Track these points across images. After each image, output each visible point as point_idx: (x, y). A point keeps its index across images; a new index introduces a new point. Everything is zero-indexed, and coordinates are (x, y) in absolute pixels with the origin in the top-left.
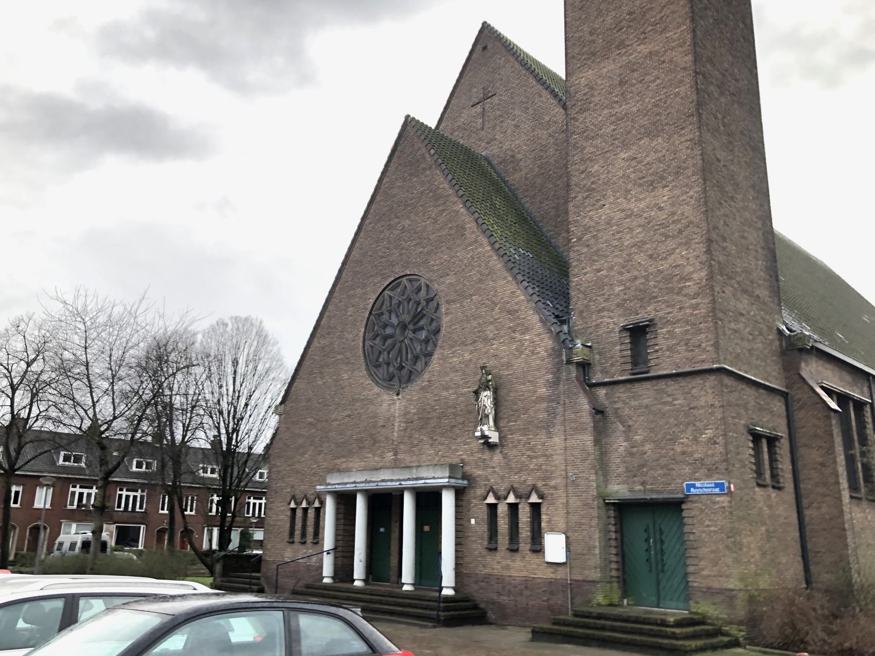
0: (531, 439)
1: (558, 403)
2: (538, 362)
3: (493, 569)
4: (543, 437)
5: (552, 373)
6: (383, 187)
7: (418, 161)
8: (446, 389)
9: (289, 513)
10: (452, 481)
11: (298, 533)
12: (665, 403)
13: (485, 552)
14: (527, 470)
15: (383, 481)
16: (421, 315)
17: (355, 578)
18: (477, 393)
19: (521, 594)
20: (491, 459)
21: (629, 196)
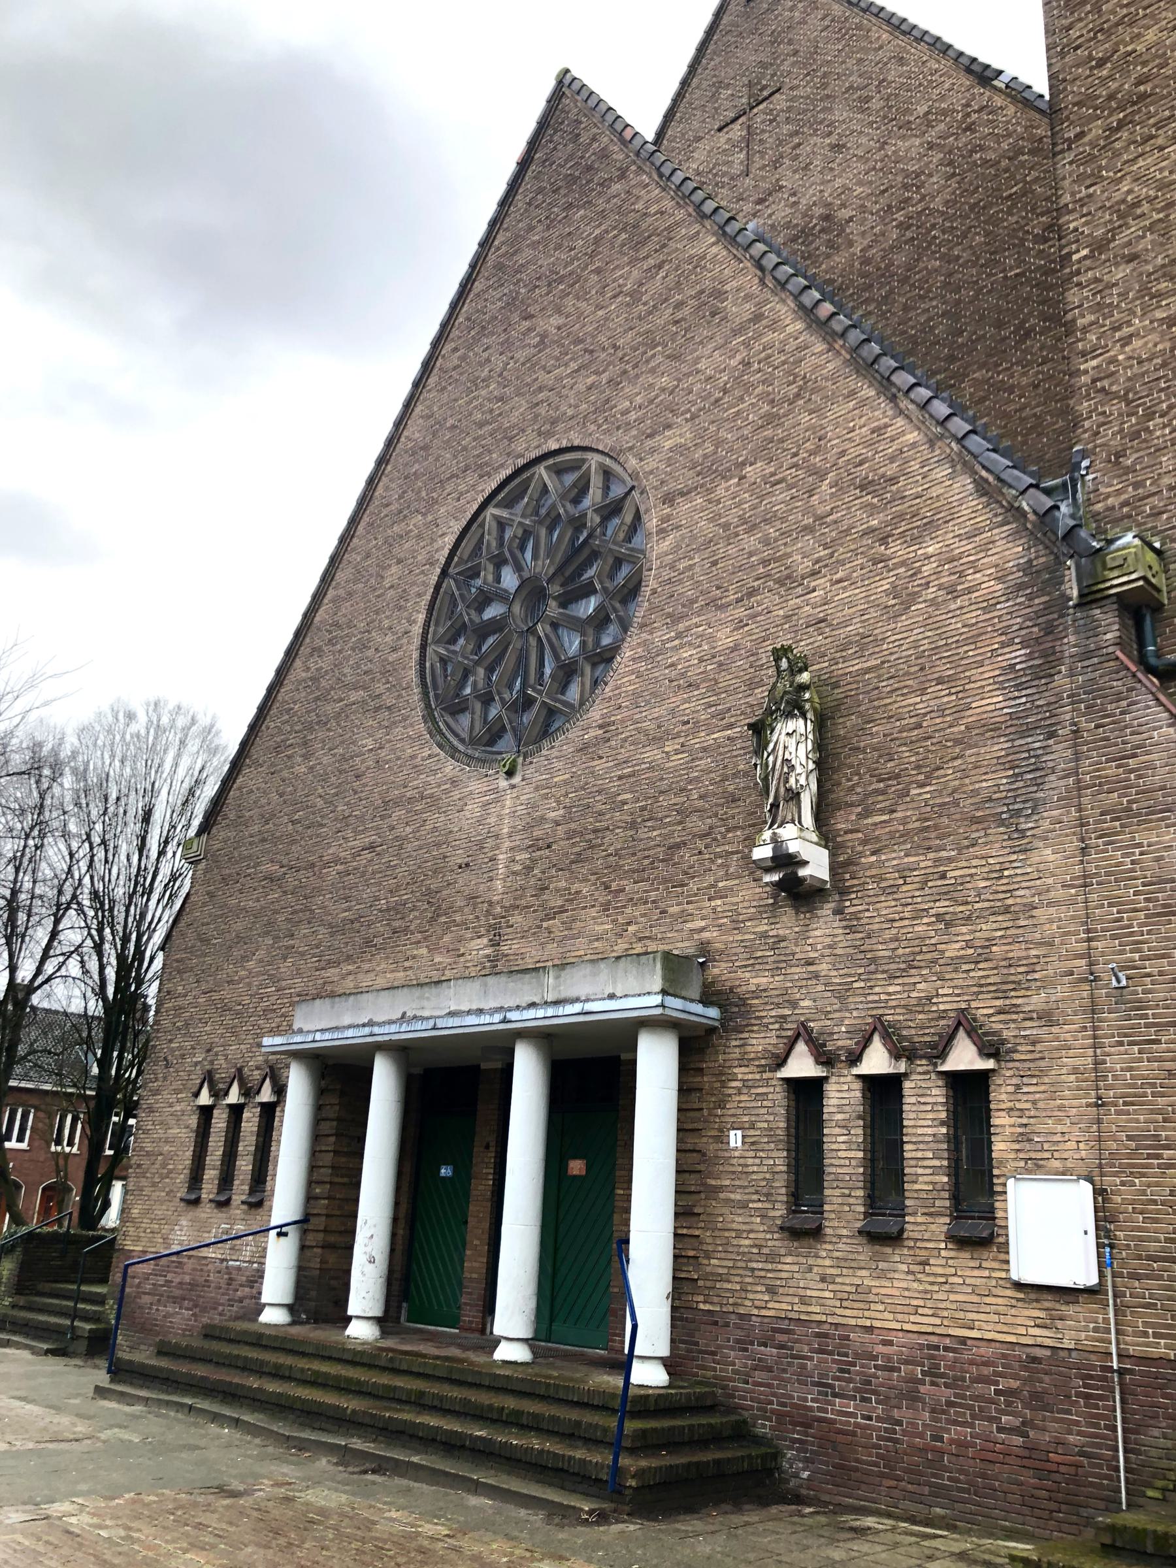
0: (950, 860)
2: (971, 617)
3: (804, 1300)
5: (1024, 644)
6: (492, 258)
7: (589, 168)
8: (657, 740)
10: (674, 1003)
11: (211, 1175)
13: (775, 1242)
14: (934, 961)
15: (452, 1014)
16: (586, 553)
17: (350, 1312)
18: (760, 730)
19: (913, 1398)
20: (803, 935)
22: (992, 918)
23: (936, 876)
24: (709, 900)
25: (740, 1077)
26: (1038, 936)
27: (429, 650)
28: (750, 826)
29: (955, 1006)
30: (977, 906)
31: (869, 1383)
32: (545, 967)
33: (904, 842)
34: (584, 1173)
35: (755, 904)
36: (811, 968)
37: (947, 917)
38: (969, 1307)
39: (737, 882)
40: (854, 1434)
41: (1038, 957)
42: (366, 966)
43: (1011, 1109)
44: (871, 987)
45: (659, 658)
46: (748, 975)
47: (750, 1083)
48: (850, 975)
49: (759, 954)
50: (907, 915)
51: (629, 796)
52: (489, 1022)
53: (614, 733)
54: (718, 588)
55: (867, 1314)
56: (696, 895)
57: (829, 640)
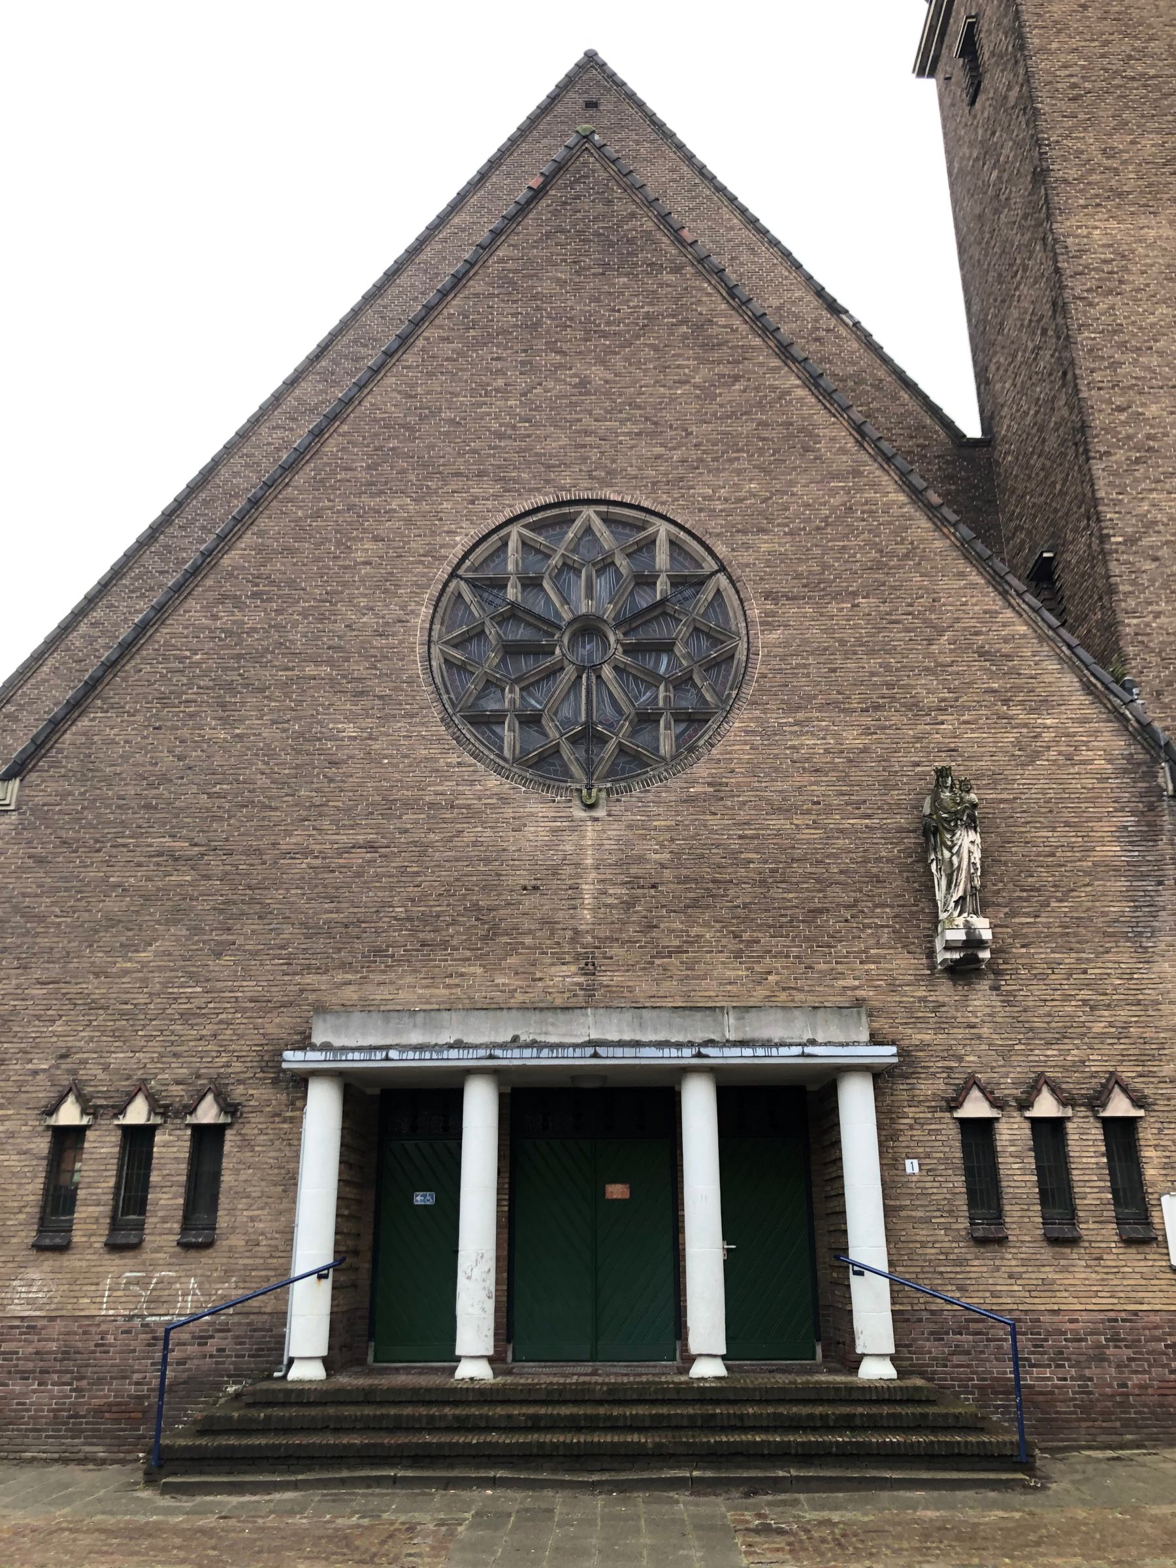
2: (1089, 782)
3: (994, 1295)
4: (1124, 958)
5: (1133, 813)
9: (42, 1145)
13: (962, 1249)
14: (1084, 1035)
19: (1101, 1359)
22: (1128, 1007)
24: (861, 963)
25: (911, 1115)
26: (1163, 1023)
27: (435, 650)
28: (899, 906)
29: (1104, 1069)
30: (1115, 997)
31: (1062, 1353)
32: (722, 1008)
33: (1049, 942)
34: (627, 1196)
35: (911, 972)
36: (973, 1031)
37: (1091, 1003)
38: (1140, 1288)
40: (1052, 1393)
42: (379, 977)
43: (1156, 1146)
44: (1031, 1050)
45: (777, 738)
46: (910, 1031)
48: (1011, 1039)
49: (920, 1014)
51: (755, 856)
52: (650, 1056)
53: (729, 794)
54: (839, 693)
55: (1053, 1300)
56: (846, 957)
57: (962, 768)
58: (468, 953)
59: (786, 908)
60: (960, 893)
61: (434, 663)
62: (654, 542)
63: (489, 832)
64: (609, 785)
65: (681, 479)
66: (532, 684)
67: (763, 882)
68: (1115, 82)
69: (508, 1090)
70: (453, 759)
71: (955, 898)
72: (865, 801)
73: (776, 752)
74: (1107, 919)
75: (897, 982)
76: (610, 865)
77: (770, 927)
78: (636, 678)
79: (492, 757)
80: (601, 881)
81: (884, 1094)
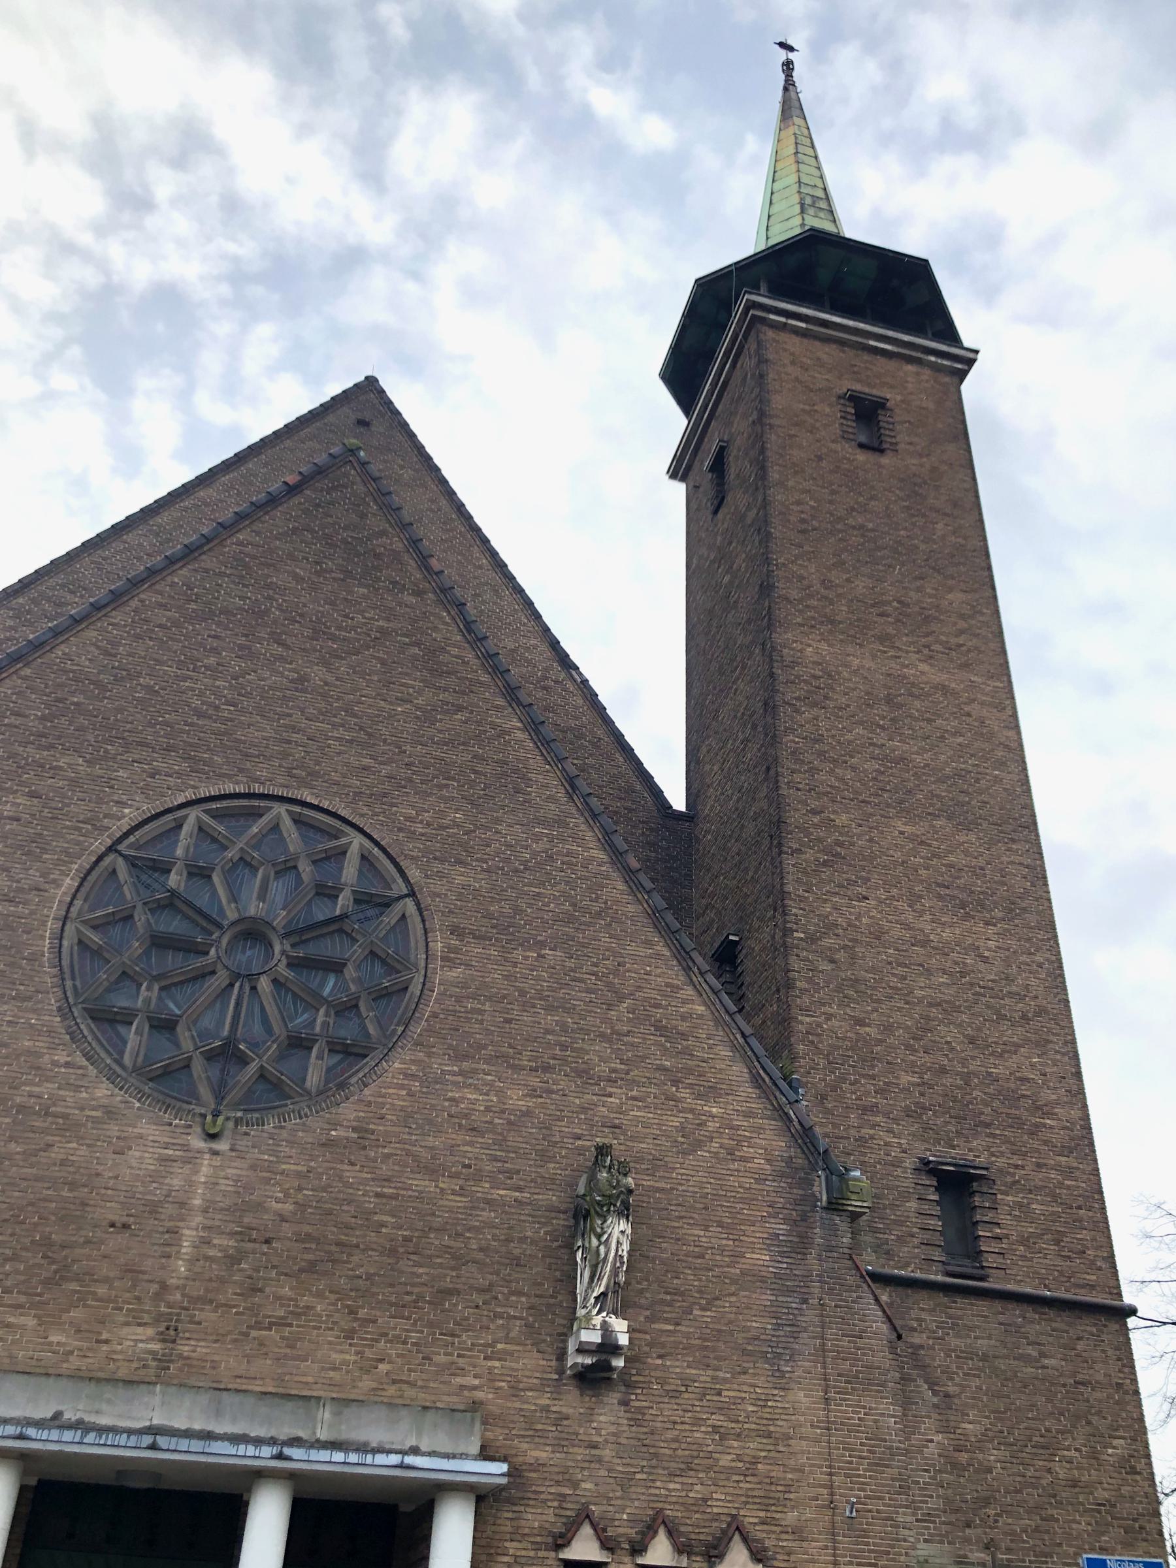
0: (725, 1380)
1: (805, 1301)
2: (747, 1181)
5: (785, 1221)
8: (431, 1171)
12: (1026, 1359)
14: (710, 1467)
20: (590, 1415)
21: (918, 906)
22: (759, 1440)
23: (713, 1392)
25: (511, 1552)
26: (792, 1462)
27: (70, 928)
28: (536, 1296)
29: (726, 1511)
30: (746, 1426)
32: (319, 1398)
33: (686, 1355)
35: (538, 1375)
36: (594, 1452)
37: (722, 1430)
39: (519, 1348)
41: (792, 1480)
44: (653, 1481)
45: (438, 1087)
46: (525, 1446)
47: (523, 1560)
49: (540, 1427)
50: (687, 1420)
52: (224, 1453)
54: (510, 1046)
56: (470, 1350)
57: (622, 1148)
58: (22, 1299)
59: (413, 1285)
60: (602, 1289)
61: (65, 943)
62: (344, 853)
63: (84, 1151)
64: (239, 1114)
65: (385, 795)
66: (175, 984)
67: (393, 1252)
68: (839, 526)
69: (33, 1482)
70: (61, 1057)
71: (595, 1294)
72: (518, 1172)
73: (433, 1102)
74: (749, 1335)
75: (521, 1386)
76: (222, 1209)
77: (392, 1304)
78: (295, 995)
79: (108, 1061)
80: (205, 1228)
81: (485, 1523)
